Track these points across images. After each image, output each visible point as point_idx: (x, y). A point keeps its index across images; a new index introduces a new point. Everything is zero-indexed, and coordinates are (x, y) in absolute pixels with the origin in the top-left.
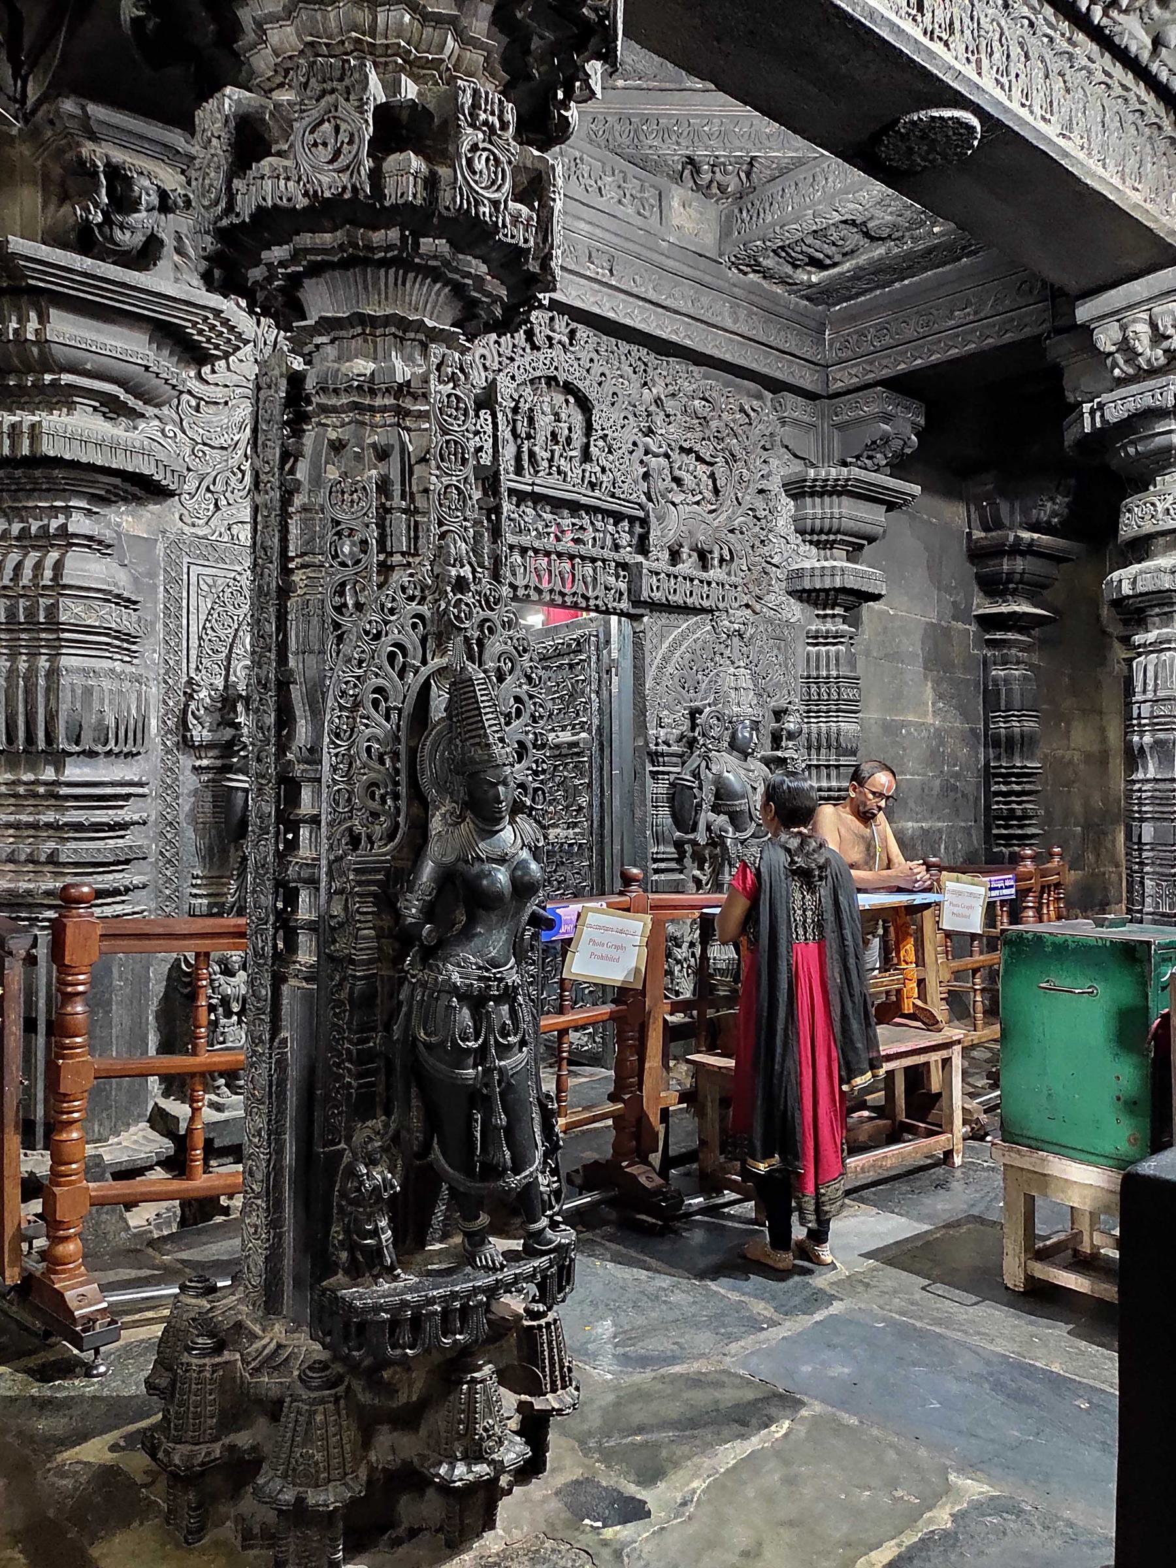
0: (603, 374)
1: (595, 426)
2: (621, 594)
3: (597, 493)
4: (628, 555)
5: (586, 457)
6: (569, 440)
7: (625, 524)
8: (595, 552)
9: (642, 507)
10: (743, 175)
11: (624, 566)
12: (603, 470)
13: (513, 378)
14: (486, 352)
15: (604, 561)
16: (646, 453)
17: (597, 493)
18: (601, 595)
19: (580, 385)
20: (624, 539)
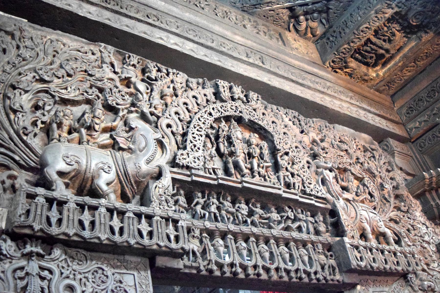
1: (278, 147)
2: (334, 269)
3: (292, 191)
4: (327, 238)
5: (277, 167)
6: (261, 156)
8: (304, 236)
10: (324, 21)
11: (329, 247)
12: (293, 175)
13: (210, 114)
14: (187, 101)
15: (313, 243)
16: (318, 167)
17: (292, 191)
18: (319, 269)
19: (260, 123)
20: (322, 228)
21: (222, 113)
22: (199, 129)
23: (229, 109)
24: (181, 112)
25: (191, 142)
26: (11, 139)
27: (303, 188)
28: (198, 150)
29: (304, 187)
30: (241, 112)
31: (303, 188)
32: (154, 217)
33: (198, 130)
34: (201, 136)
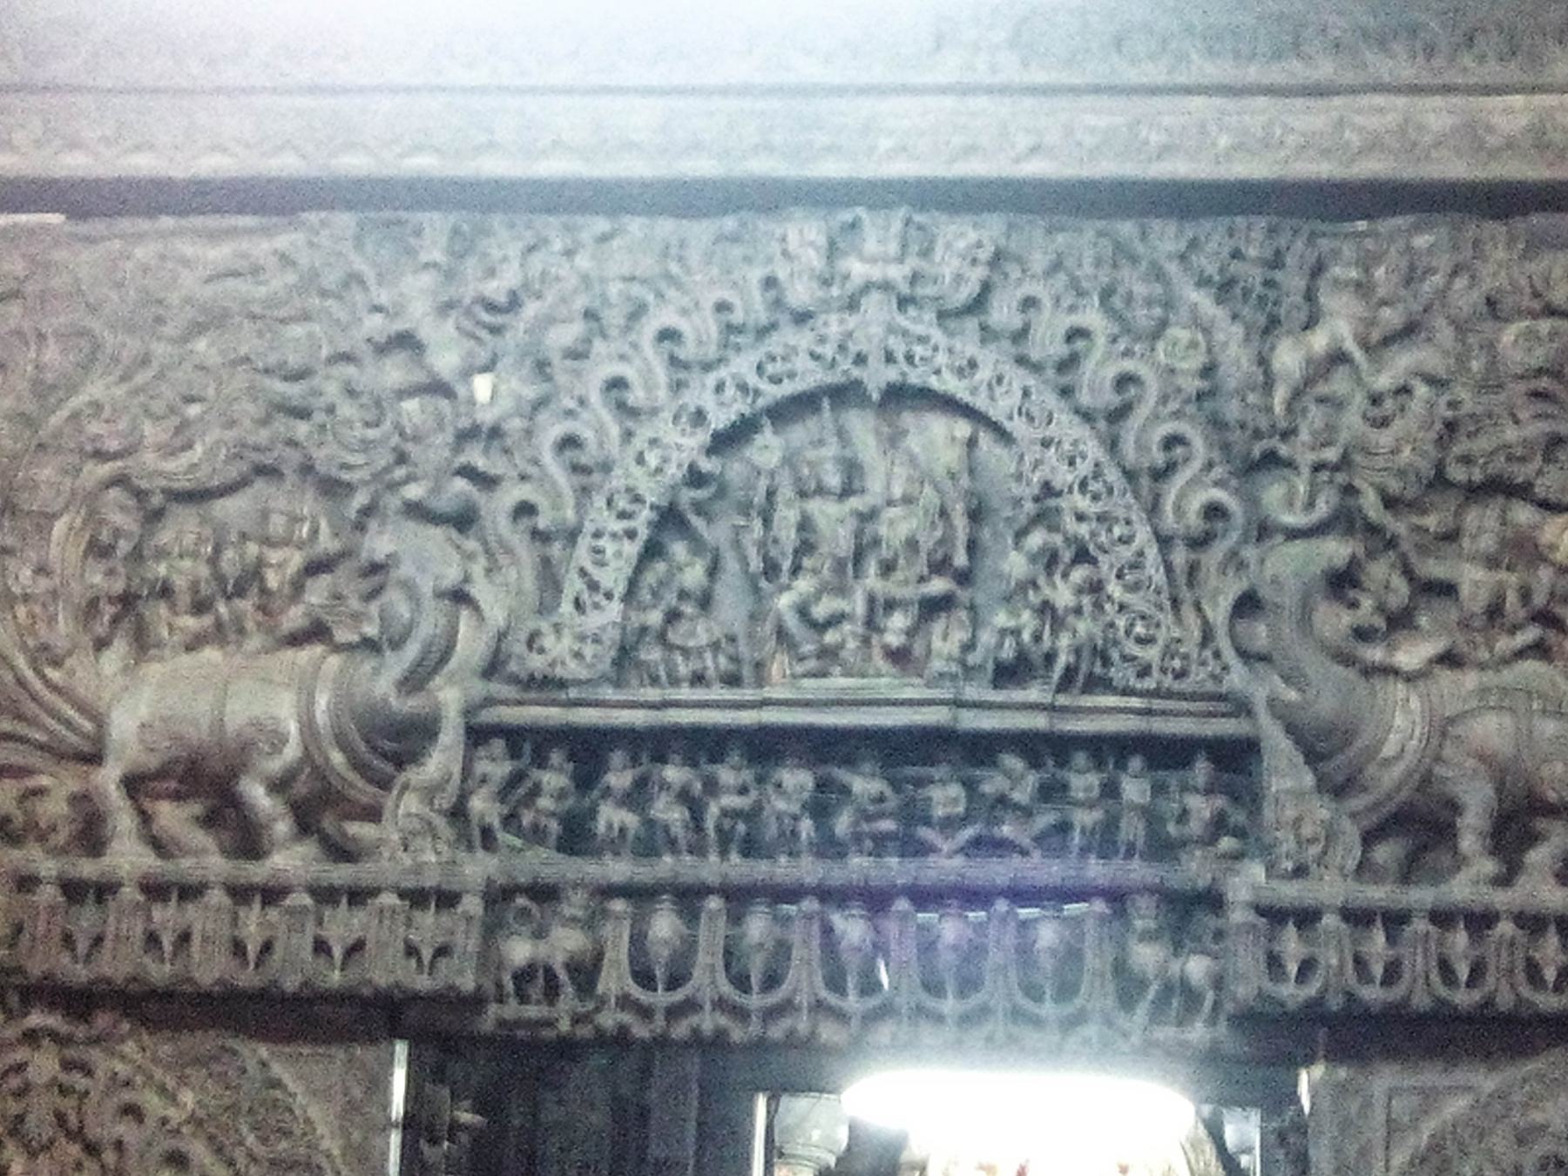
0: (1075, 334)
7: (1201, 770)
9: (1243, 708)
13: (699, 417)
17: (1034, 693)
21: (757, 393)
22: (629, 508)
23: (802, 363)
24: (588, 434)
25: (583, 572)
26: (21, 682)
27: (1098, 669)
28: (604, 602)
29: (1107, 662)
30: (860, 359)
31: (1098, 669)
32: (374, 892)
33: (623, 515)
34: (631, 534)
